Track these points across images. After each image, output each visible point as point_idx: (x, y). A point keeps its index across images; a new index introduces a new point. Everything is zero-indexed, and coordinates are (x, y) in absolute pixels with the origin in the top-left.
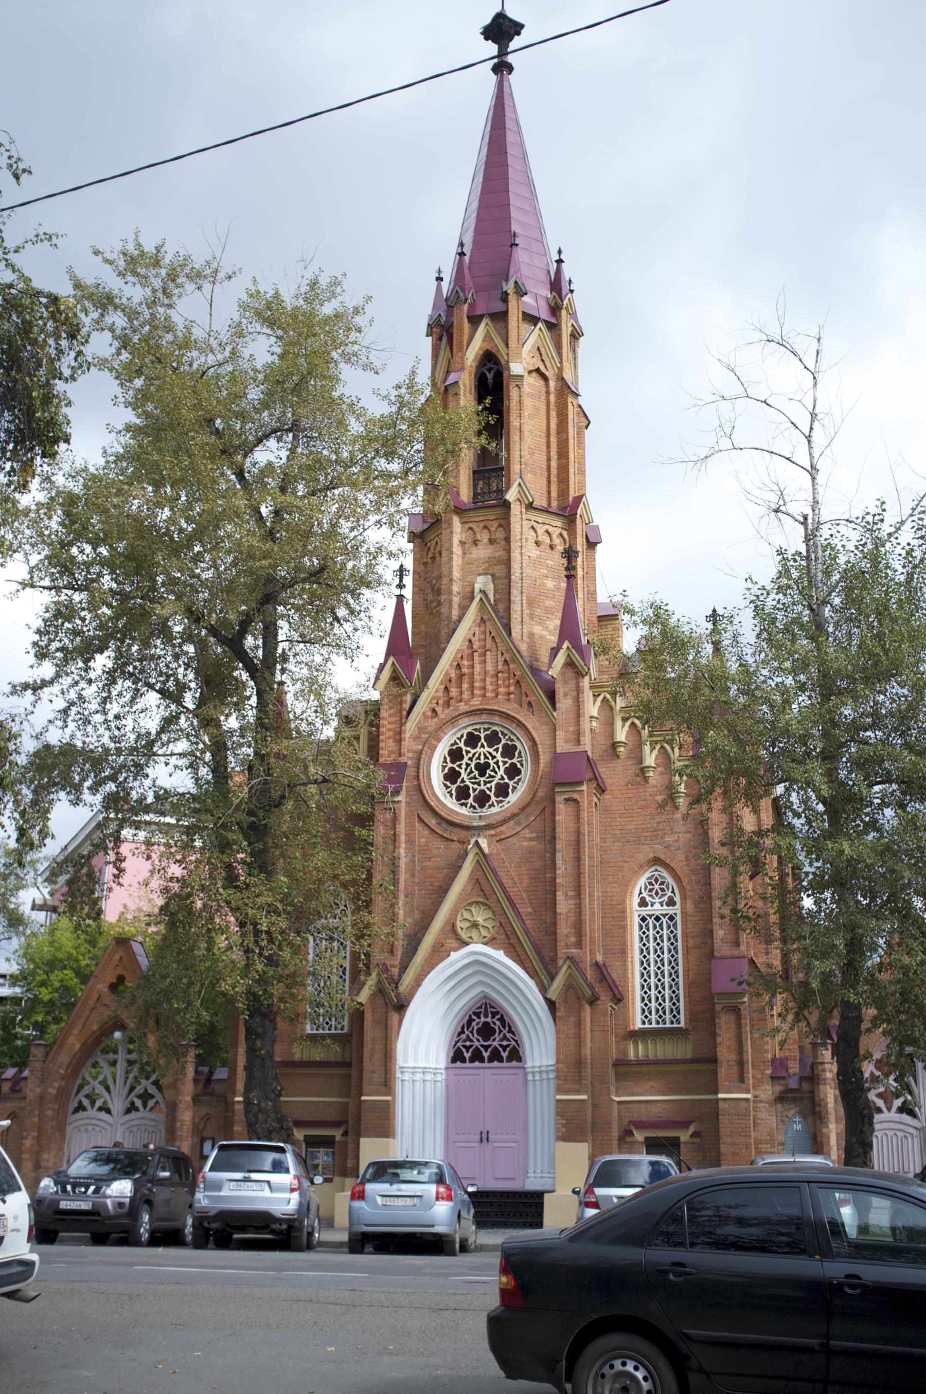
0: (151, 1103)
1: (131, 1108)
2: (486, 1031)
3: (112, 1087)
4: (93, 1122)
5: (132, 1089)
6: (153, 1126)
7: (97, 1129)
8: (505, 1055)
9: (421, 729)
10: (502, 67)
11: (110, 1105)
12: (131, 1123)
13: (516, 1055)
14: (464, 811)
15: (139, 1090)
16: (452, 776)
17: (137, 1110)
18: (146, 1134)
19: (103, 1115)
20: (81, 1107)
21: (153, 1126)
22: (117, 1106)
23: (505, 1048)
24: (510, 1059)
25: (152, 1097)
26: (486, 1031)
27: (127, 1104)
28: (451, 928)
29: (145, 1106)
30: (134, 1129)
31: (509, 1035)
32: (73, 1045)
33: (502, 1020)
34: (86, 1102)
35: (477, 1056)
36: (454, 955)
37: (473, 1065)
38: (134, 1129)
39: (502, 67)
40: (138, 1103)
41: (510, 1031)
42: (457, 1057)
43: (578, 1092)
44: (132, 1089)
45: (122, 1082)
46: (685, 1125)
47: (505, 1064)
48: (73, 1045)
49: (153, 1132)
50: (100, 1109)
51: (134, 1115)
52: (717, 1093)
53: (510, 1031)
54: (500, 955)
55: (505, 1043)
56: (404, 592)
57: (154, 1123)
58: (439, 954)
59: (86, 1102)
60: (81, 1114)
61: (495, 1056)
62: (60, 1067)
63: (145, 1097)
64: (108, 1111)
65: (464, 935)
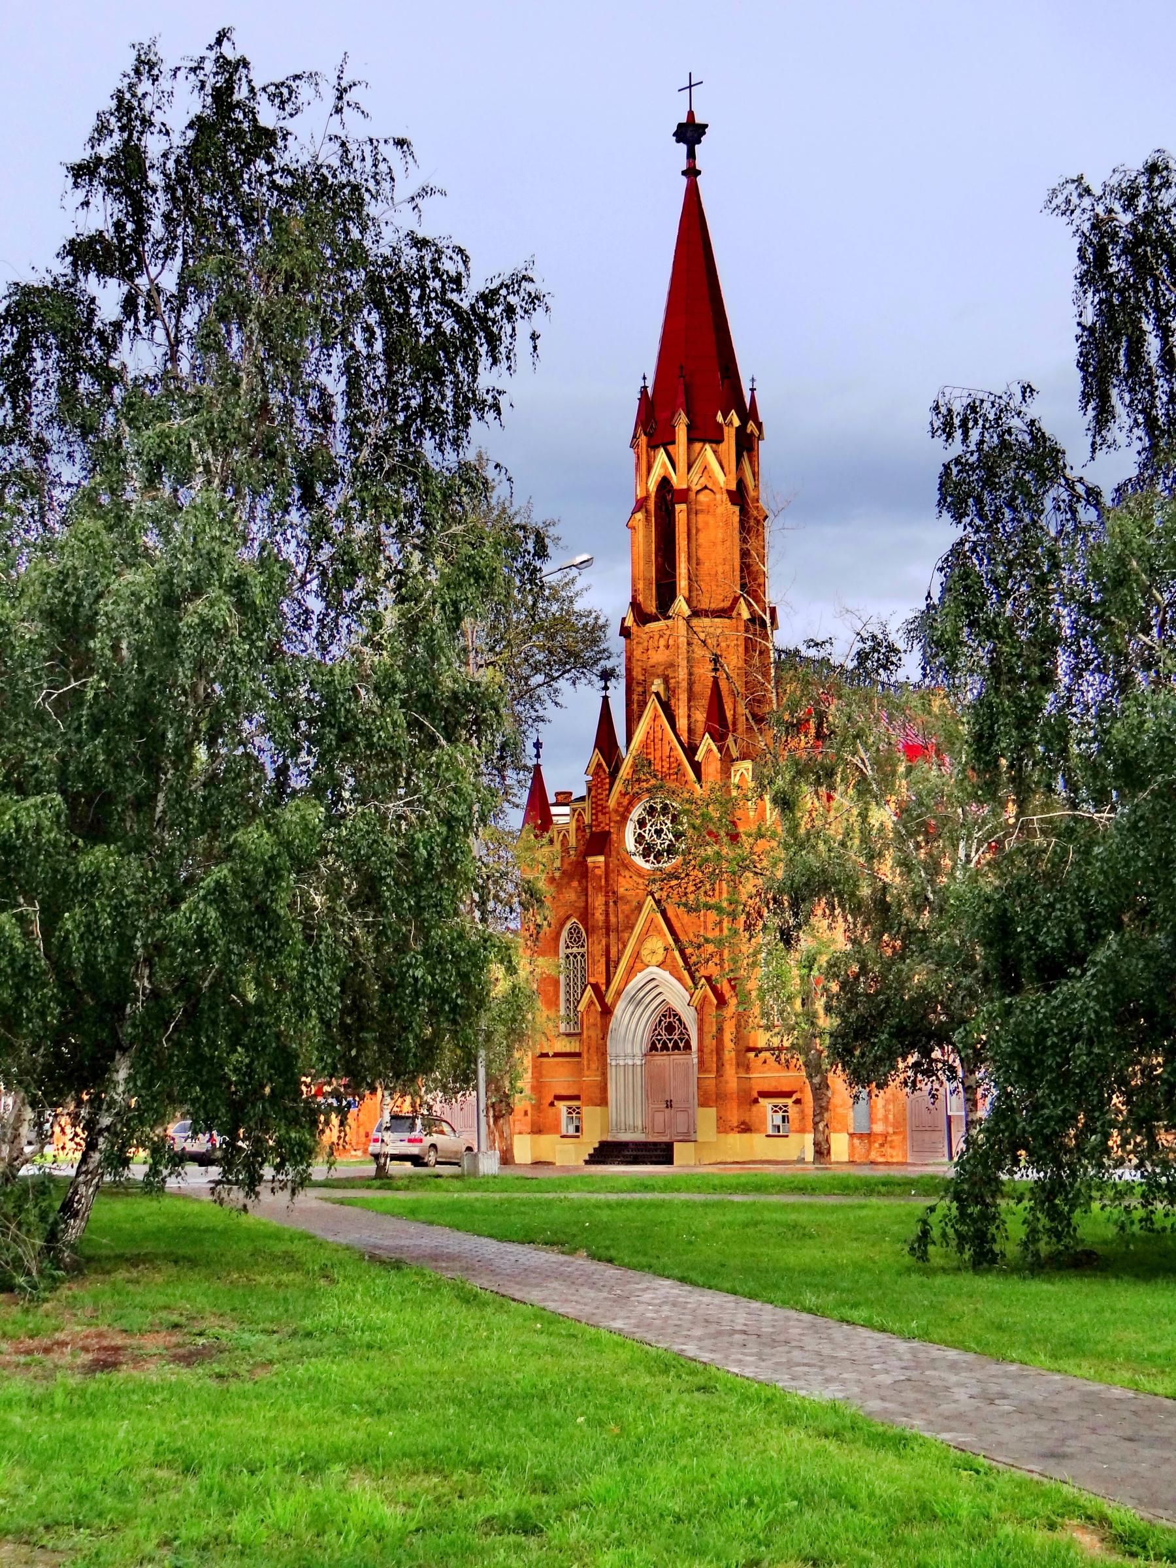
2: (670, 1029)
9: (619, 804)
10: (692, 173)
14: (648, 866)
16: (639, 839)
26: (670, 1029)
28: (637, 955)
33: (680, 1020)
35: (665, 1047)
36: (639, 975)
39: (692, 173)
42: (653, 1047)
46: (788, 1095)
54: (666, 974)
56: (609, 693)
58: (631, 972)
61: (676, 1047)
65: (646, 959)
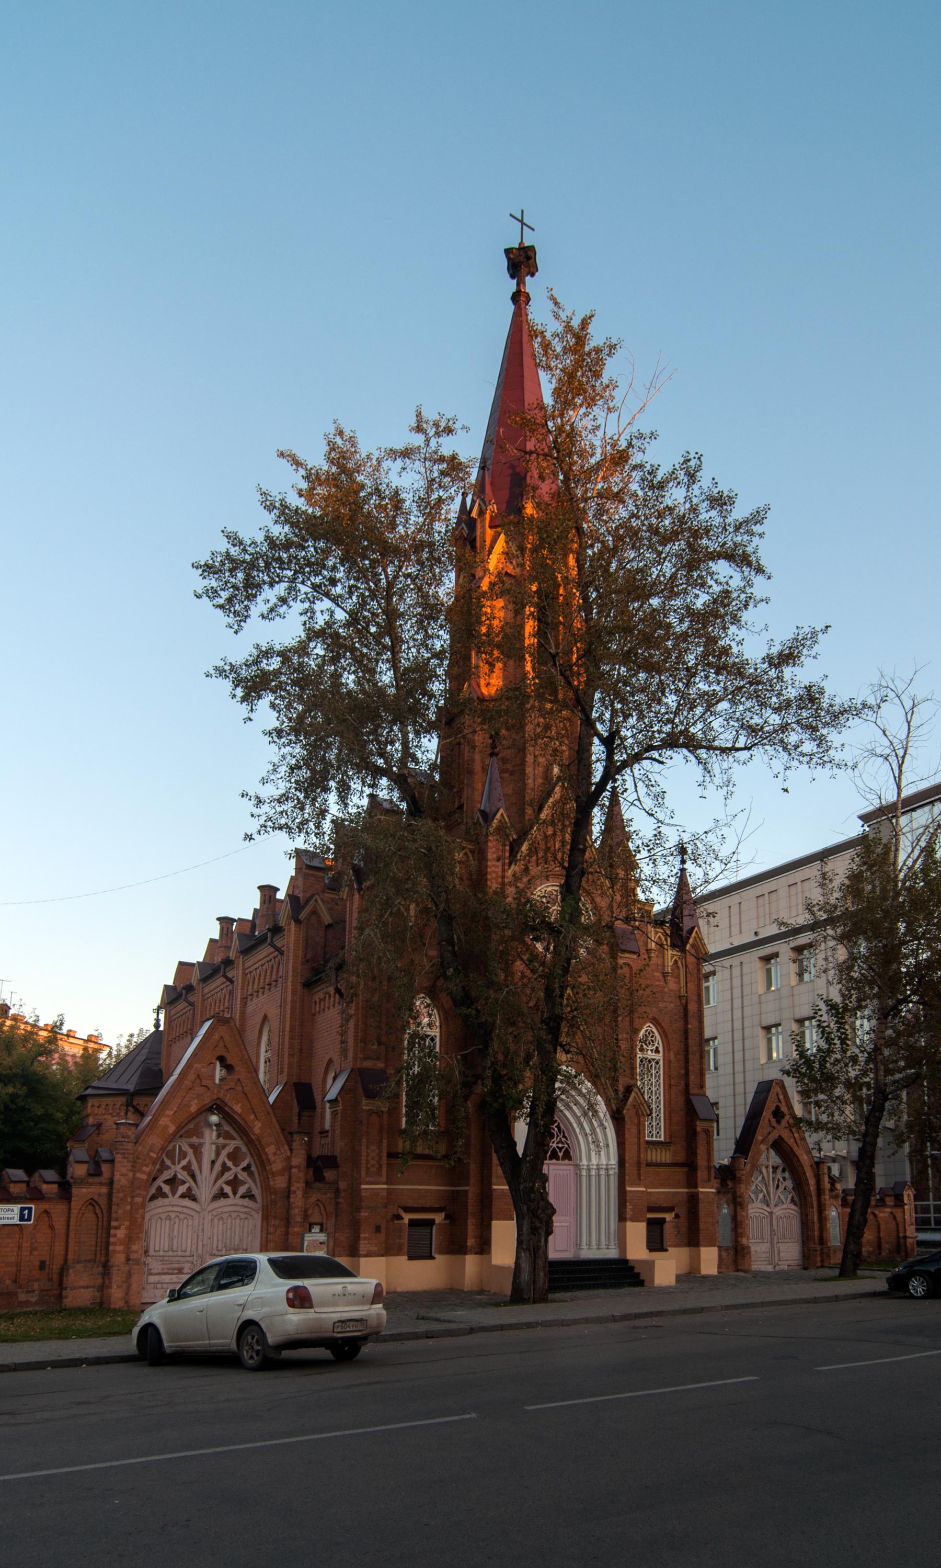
0: (242, 1190)
1: (222, 1195)
3: (197, 1172)
4: (175, 1209)
5: (222, 1173)
6: (245, 1213)
7: (182, 1216)
8: (561, 1154)
11: (195, 1191)
12: (220, 1210)
13: (567, 1156)
15: (228, 1176)
17: (225, 1196)
18: (238, 1221)
19: (187, 1202)
20: (160, 1194)
21: (245, 1213)
22: (205, 1190)
23: (560, 1149)
24: (564, 1158)
25: (244, 1183)
27: (215, 1190)
29: (235, 1193)
30: (225, 1216)
31: (563, 1139)
32: (166, 1127)
34: (166, 1189)
37: (551, 1162)
38: (225, 1216)
40: (228, 1190)
41: (564, 1136)
43: (639, 1186)
44: (222, 1173)
45: (209, 1169)
47: (560, 1162)
48: (166, 1127)
49: (246, 1218)
50: (183, 1196)
51: (223, 1202)
52: (696, 1187)
53: (564, 1136)
55: (560, 1145)
57: (246, 1210)
59: (166, 1189)
60: (160, 1201)
62: (151, 1150)
63: (235, 1183)
64: (194, 1199)
